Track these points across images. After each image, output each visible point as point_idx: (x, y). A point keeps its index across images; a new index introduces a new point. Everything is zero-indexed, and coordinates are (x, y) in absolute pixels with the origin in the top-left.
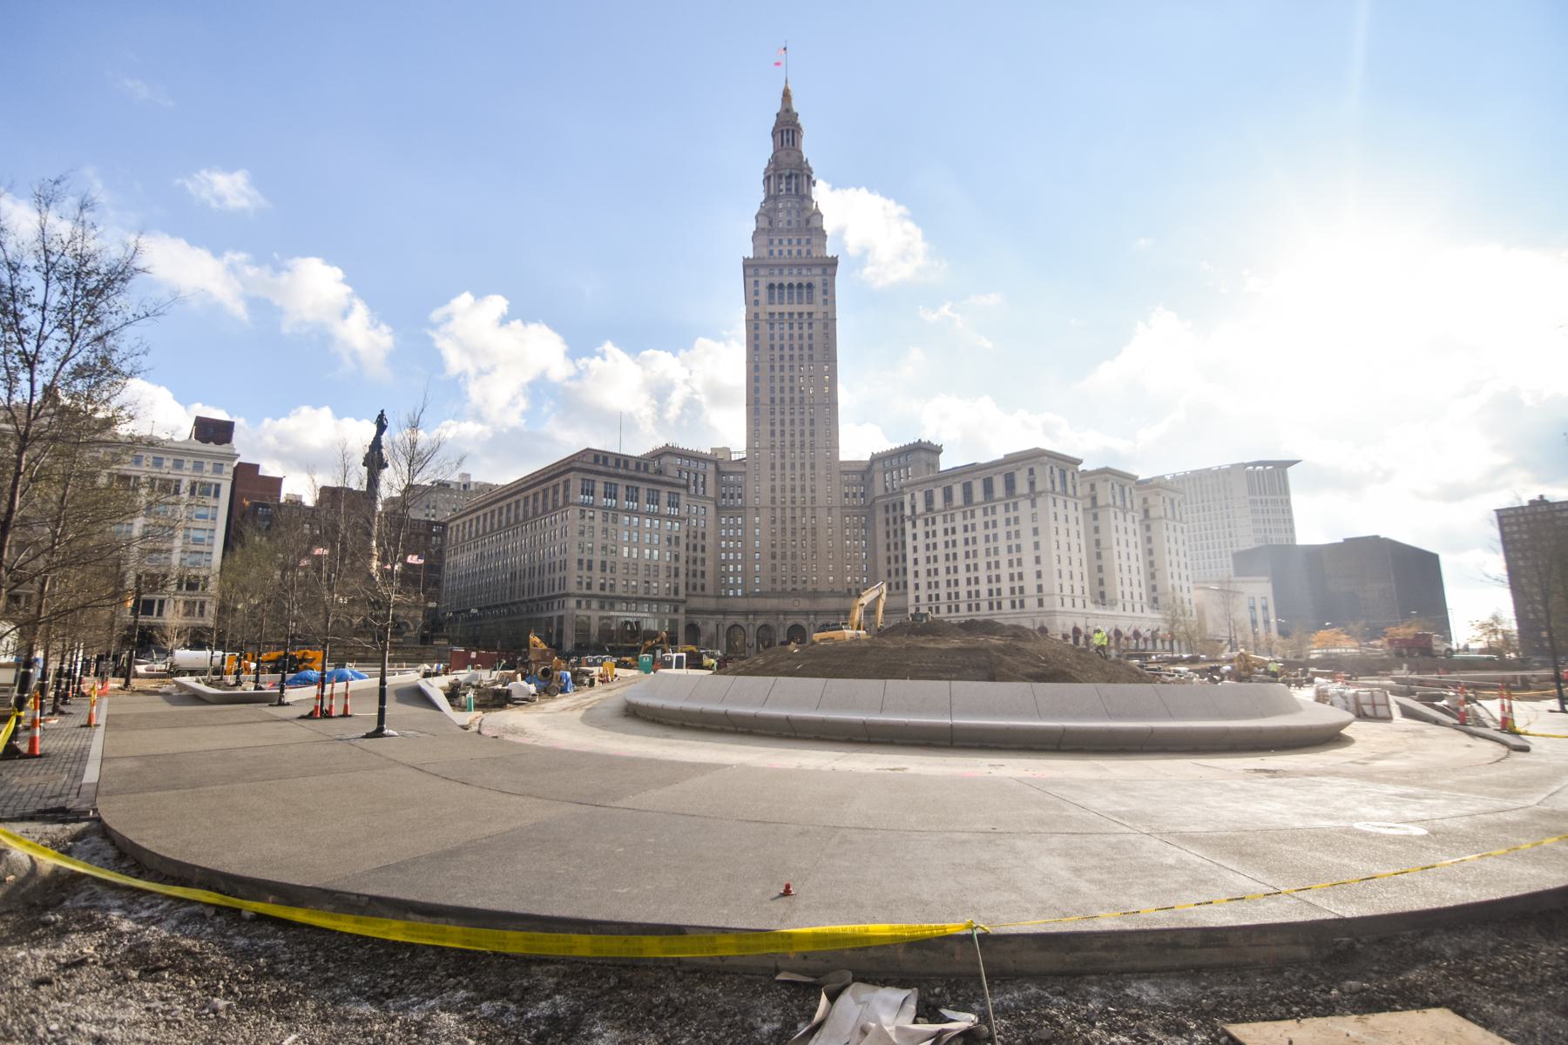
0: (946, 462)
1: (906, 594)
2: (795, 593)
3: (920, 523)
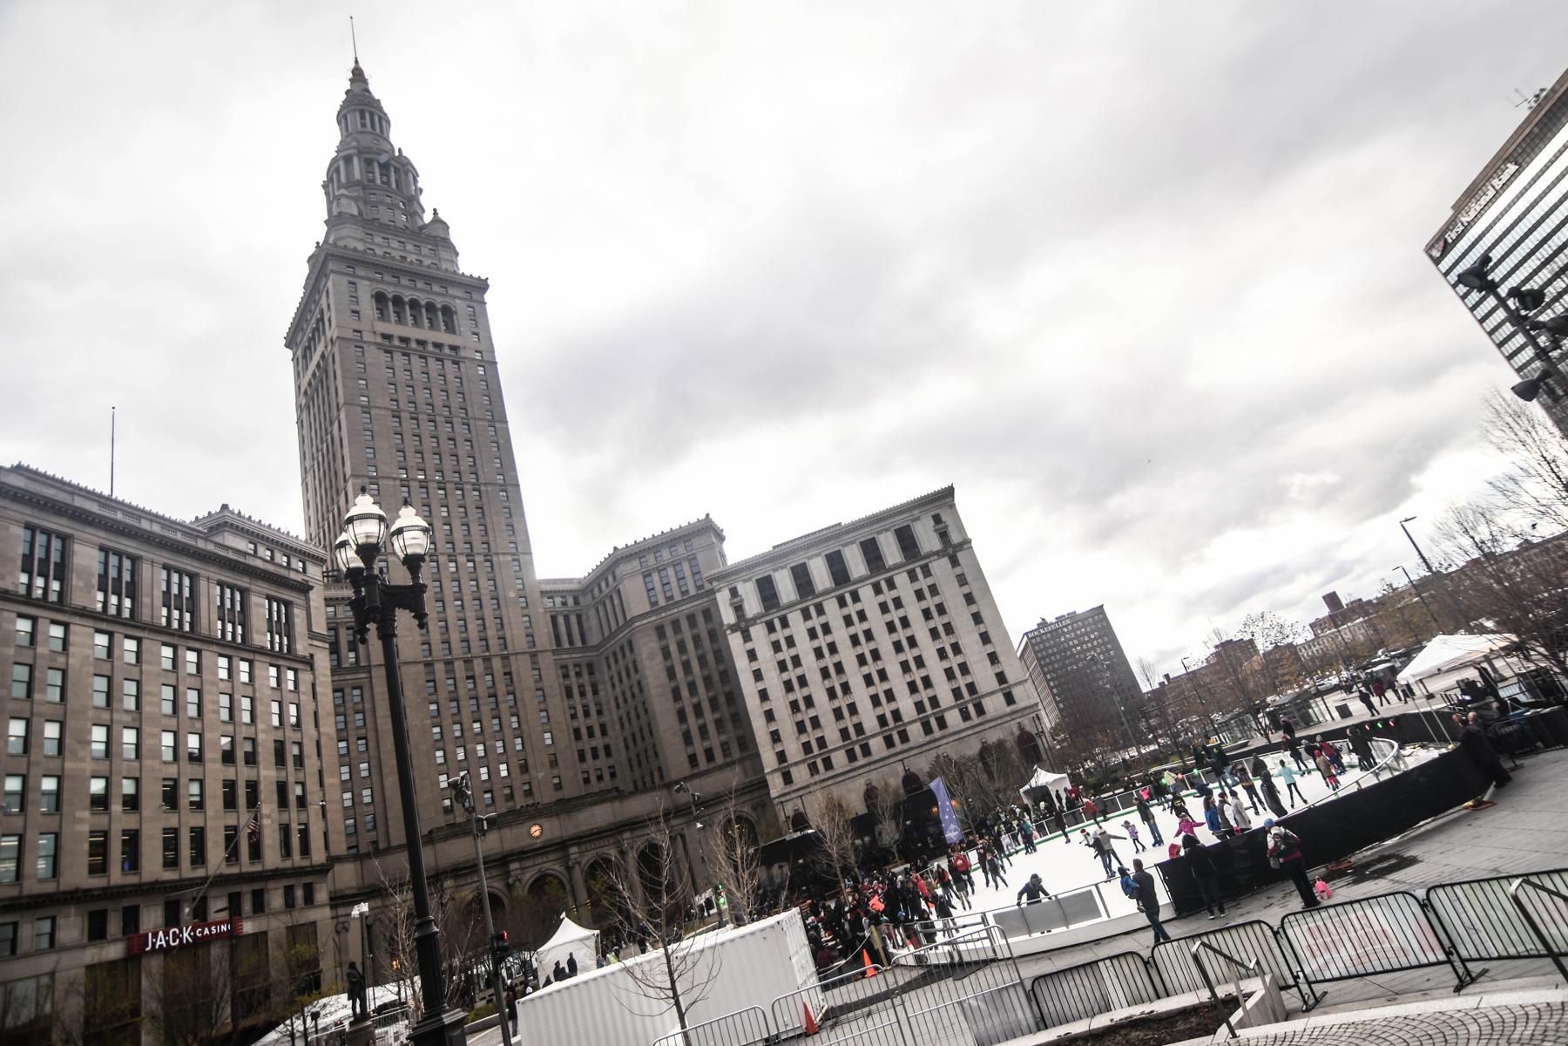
0: (737, 551)
1: (758, 755)
2: (534, 813)
3: (758, 631)
